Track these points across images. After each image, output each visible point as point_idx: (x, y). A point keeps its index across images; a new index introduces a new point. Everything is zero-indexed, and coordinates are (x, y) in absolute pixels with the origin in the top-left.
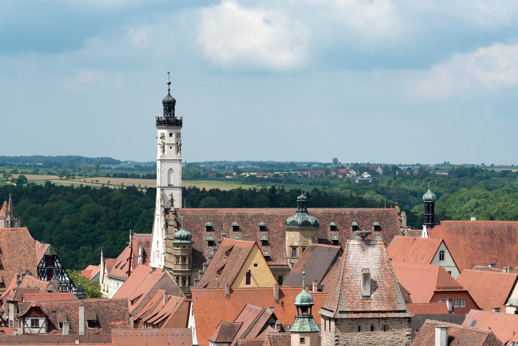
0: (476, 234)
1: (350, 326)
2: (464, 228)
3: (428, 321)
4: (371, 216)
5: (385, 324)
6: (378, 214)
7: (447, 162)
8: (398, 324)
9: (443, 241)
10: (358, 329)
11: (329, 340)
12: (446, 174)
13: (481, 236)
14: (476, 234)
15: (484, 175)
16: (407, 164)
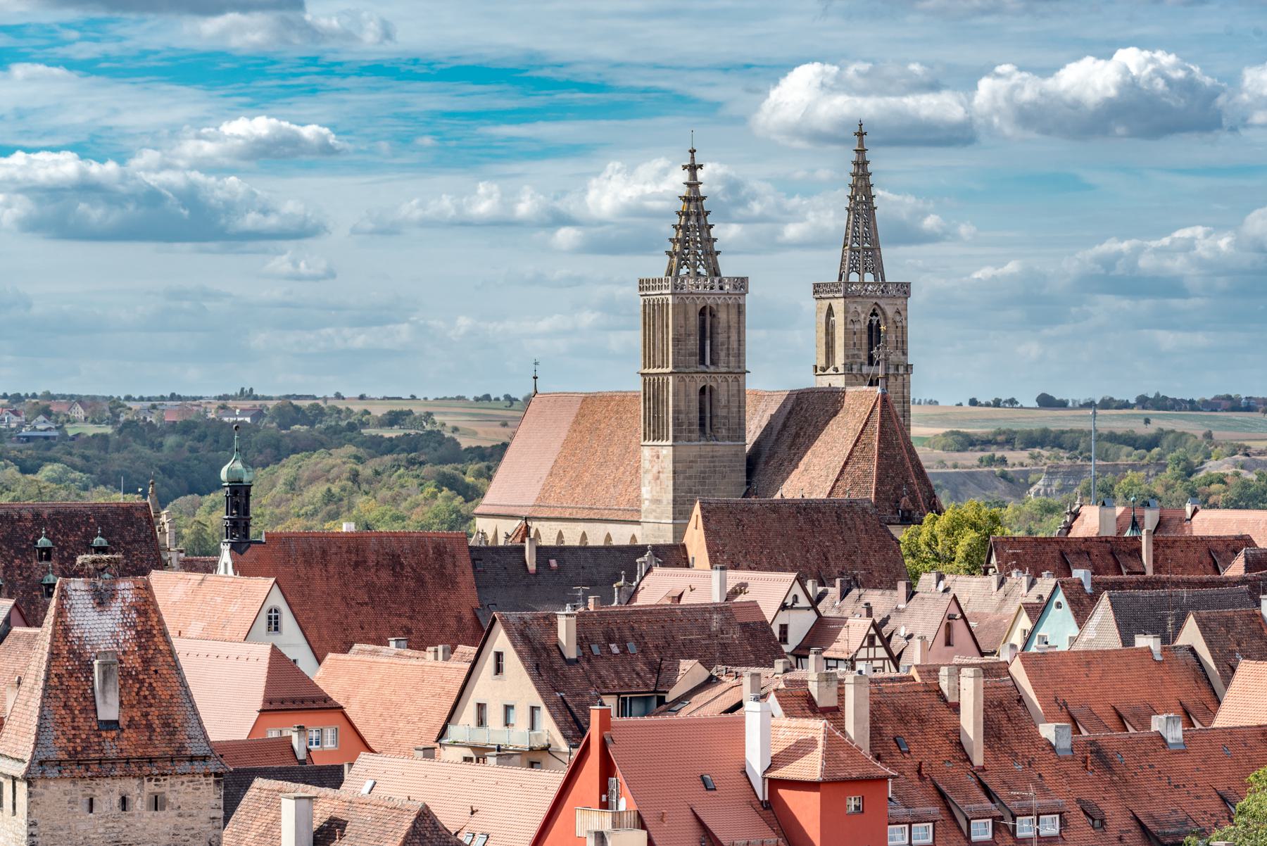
0: (357, 564)
1: (68, 798)
2: (324, 552)
3: (258, 782)
4: (87, 524)
5: (157, 790)
6: (105, 516)
7: (247, 389)
8: (190, 790)
9: (276, 581)
10: (86, 806)
11: (11, 835)
12: (248, 420)
13: (367, 569)
14: (357, 564)
15: (344, 423)
16: (145, 396)
